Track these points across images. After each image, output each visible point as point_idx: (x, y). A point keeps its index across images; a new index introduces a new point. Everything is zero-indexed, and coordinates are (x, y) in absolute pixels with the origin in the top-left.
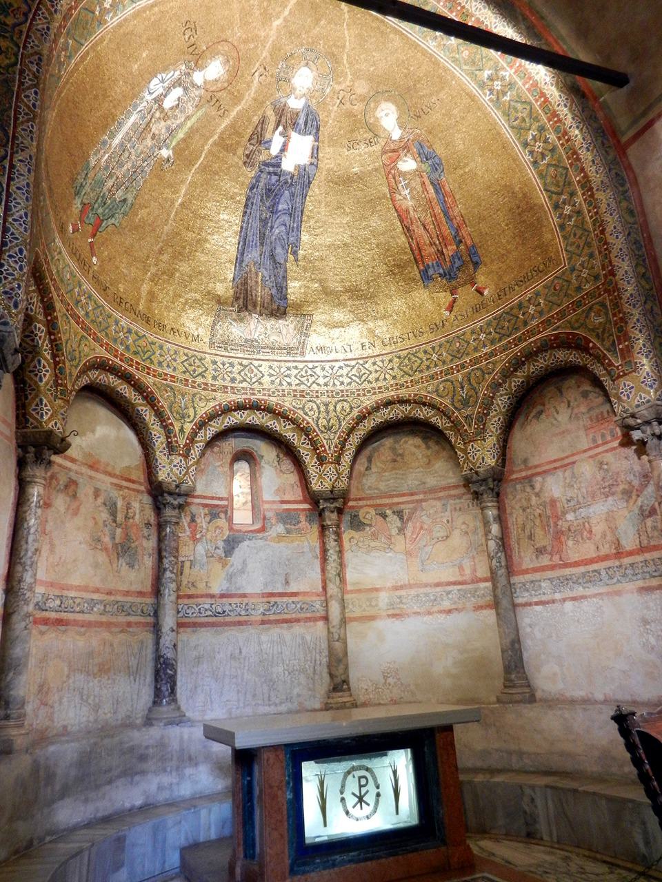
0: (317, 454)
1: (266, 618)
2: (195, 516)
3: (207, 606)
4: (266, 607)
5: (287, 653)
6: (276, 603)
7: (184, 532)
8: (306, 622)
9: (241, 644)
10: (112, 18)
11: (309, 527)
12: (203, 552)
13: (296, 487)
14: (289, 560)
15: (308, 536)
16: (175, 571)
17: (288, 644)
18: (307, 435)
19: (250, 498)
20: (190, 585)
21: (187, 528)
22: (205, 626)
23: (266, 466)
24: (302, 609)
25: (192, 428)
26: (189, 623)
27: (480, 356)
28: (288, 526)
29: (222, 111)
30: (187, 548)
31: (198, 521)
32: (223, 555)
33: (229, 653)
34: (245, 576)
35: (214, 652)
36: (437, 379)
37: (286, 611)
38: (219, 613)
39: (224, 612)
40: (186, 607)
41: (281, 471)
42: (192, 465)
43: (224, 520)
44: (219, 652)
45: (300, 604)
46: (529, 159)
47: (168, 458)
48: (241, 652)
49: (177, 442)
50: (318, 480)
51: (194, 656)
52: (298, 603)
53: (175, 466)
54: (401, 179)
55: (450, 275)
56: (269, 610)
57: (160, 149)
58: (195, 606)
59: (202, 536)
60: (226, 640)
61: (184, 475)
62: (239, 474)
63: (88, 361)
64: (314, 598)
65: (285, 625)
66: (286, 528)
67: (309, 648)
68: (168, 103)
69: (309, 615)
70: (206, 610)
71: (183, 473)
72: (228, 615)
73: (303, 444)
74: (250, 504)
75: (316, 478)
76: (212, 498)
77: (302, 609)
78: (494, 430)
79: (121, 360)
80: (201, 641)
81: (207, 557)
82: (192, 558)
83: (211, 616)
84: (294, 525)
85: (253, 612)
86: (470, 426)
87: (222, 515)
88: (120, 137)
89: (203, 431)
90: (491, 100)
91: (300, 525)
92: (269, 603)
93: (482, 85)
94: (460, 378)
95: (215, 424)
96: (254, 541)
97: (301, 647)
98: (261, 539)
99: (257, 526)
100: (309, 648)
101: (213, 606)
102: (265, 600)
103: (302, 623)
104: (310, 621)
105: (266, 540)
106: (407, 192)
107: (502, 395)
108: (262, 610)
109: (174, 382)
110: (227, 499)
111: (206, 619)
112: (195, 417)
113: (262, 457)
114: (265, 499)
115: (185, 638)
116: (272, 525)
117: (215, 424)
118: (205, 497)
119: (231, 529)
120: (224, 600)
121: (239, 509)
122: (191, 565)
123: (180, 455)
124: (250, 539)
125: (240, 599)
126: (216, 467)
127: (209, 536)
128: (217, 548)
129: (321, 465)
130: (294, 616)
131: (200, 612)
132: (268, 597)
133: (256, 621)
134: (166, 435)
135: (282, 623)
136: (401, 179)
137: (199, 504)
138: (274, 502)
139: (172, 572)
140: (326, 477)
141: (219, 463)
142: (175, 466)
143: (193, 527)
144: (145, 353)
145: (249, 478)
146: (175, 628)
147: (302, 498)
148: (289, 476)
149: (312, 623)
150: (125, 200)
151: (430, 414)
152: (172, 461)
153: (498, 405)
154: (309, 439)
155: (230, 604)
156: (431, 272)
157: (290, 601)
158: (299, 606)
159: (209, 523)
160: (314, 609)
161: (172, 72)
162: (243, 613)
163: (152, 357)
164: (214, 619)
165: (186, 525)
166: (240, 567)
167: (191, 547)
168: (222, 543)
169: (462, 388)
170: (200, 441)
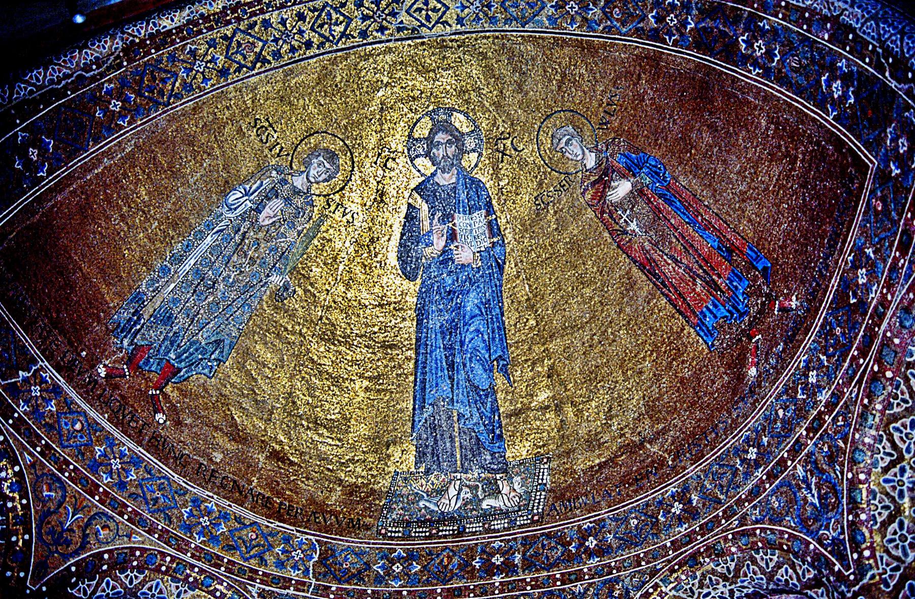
10: (130, 123)
27: (820, 413)
29: (350, 215)
36: (765, 490)
46: (758, 74)
54: (620, 212)
55: (738, 311)
57: (268, 276)
63: (110, 552)
68: (265, 218)
78: (899, 553)
79: (193, 556)
86: (842, 558)
88: (192, 262)
90: (675, 43)
93: (655, 35)
94: (800, 471)
106: (633, 226)
107: (886, 470)
109: (303, 591)
136: (620, 212)
144: (249, 549)
150: (218, 342)
151: (771, 565)
153: (887, 494)
156: (709, 321)
161: (259, 182)
163: (267, 556)
169: (809, 487)
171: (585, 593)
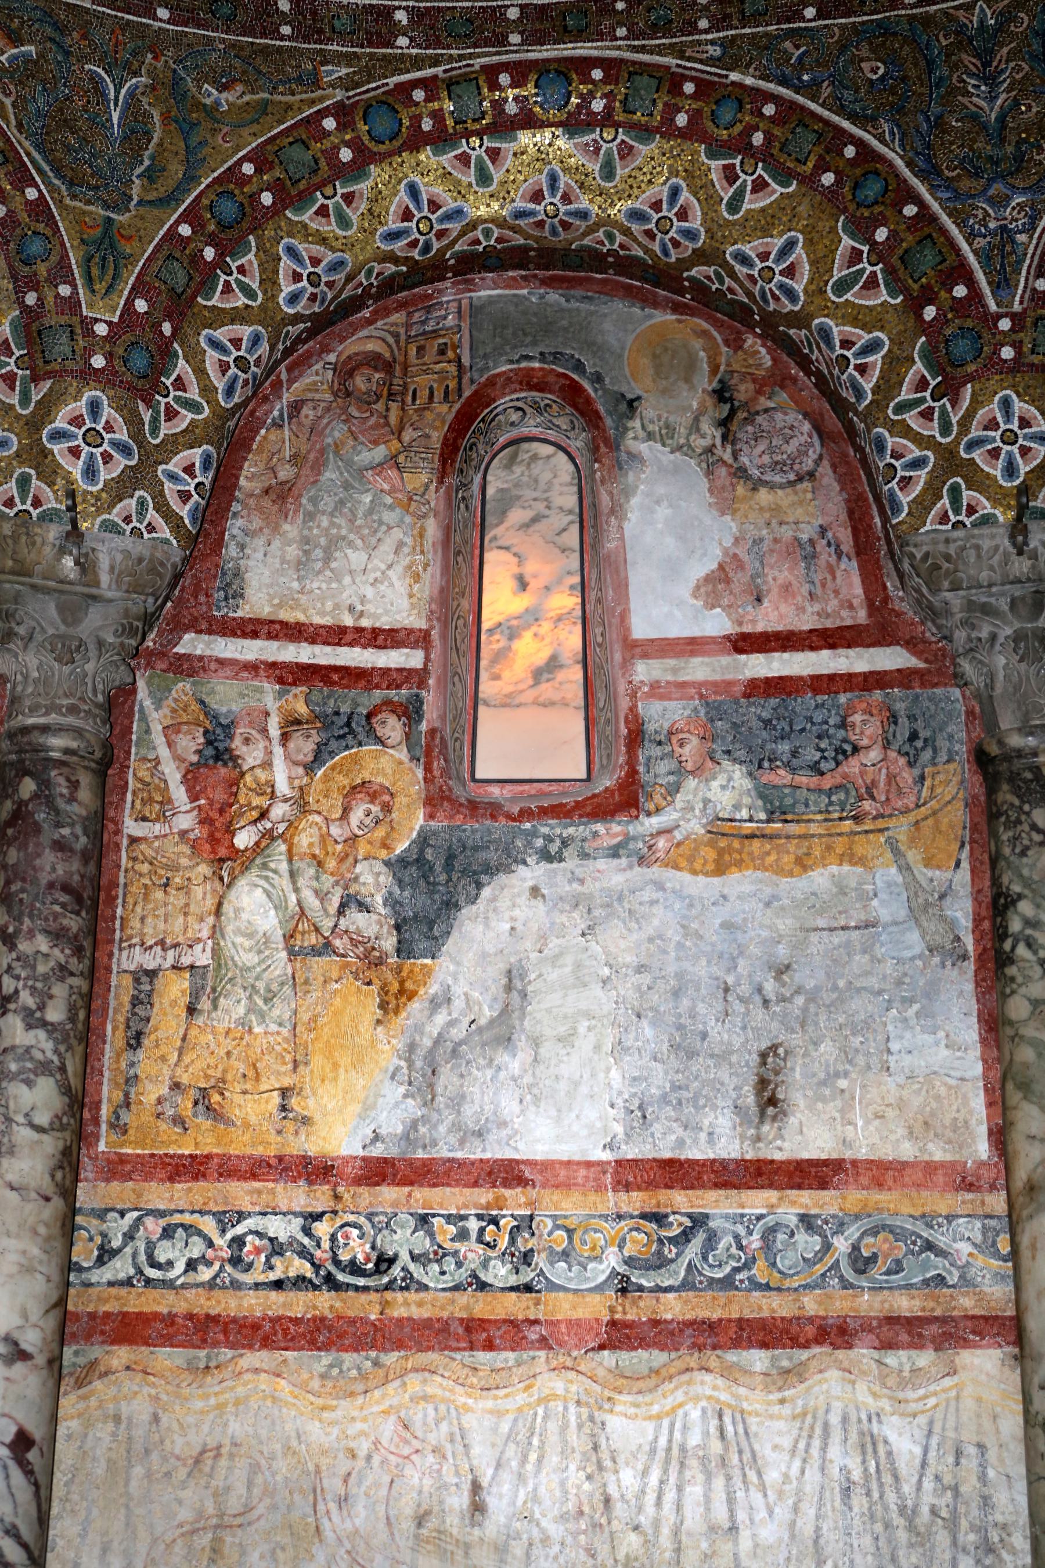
0: (924, 327)
1: (635, 1312)
2: (228, 729)
3: (281, 1228)
4: (637, 1243)
5: (769, 1532)
6: (699, 1221)
7: (162, 817)
8: (888, 1345)
9: (482, 1456)
11: (907, 776)
12: (269, 922)
13: (826, 555)
14: (782, 971)
15: (901, 828)
16: (55, 1014)
17: (772, 1476)
18: (862, 229)
19: (573, 640)
20: (186, 1105)
21: (179, 794)
22: (267, 1343)
23: (644, 448)
24: (862, 1263)
25: (172, 234)
26: (170, 1319)
28: (783, 777)
30: (176, 899)
31: (251, 756)
32: (389, 943)
33: (407, 1507)
34: (514, 1063)
35: (316, 1493)
37: (760, 1271)
38: (353, 1267)
39: (385, 1262)
40: (153, 1226)
41: (741, 473)
42: (173, 445)
43: (402, 754)
44: (343, 1501)
45: (853, 1232)
47: (25, 399)
48: (478, 1508)
49: (72, 304)
50: (933, 491)
51: (185, 1514)
52: (841, 1227)
53: (58, 435)
56: (660, 1263)
58: (208, 1225)
59: (269, 836)
60: (388, 1428)
61: (120, 489)
62: (517, 515)
64: (943, 1203)
65: (758, 1359)
66: (764, 793)
67: (910, 1514)
69: (905, 1305)
70: (276, 1248)
71: (105, 474)
72: (409, 1283)
73: (842, 287)
74: (576, 674)
75: (922, 475)
76: (336, 636)
77: (862, 1263)
80: (235, 1427)
81: (292, 954)
82: (202, 957)
83: (300, 1282)
84: (816, 769)
85: (559, 1272)
87: (392, 728)
89: (250, 257)
91: (852, 766)
92: (658, 1218)
95: (330, 227)
96: (571, 863)
97: (858, 1502)
98: (614, 852)
99: (606, 782)
100: (910, 1514)
101: (323, 1229)
102: (635, 1201)
103: (863, 1354)
104: (916, 1344)
105: (642, 860)
108: (612, 1260)
110: (420, 639)
111: (277, 1303)
112: (191, 179)
113: (632, 404)
114: (641, 629)
115: (139, 1409)
116: (680, 771)
117: (330, 227)
118: (295, 632)
119: (433, 802)
120: (389, 1194)
121: (507, 702)
122: (196, 994)
123: (88, 375)
124: (547, 856)
125: (484, 1195)
126: (361, 471)
127: (306, 839)
128: (351, 902)
129: (949, 389)
130: (811, 1305)
131: (236, 1261)
132: (650, 1185)
133: (573, 1324)
134: (14, 277)
135: (737, 1344)
137: (252, 668)
138: (693, 646)
139: (33, 1020)
140: (978, 456)
141: (381, 452)
142: (58, 435)
143: (220, 795)
145: (572, 538)
146: (31, 1340)
147: (862, 616)
148: (783, 497)
149: (925, 1358)
152: (46, 409)
154: (878, 253)
155: (423, 1220)
157: (789, 1214)
158: (841, 1245)
159: (310, 768)
160: (938, 1265)
162: (500, 1273)
164: (325, 1302)
165: (172, 774)
166: (487, 1013)
167: (202, 896)
168: (386, 879)
170: (238, 316)
171: (1000, 28)
